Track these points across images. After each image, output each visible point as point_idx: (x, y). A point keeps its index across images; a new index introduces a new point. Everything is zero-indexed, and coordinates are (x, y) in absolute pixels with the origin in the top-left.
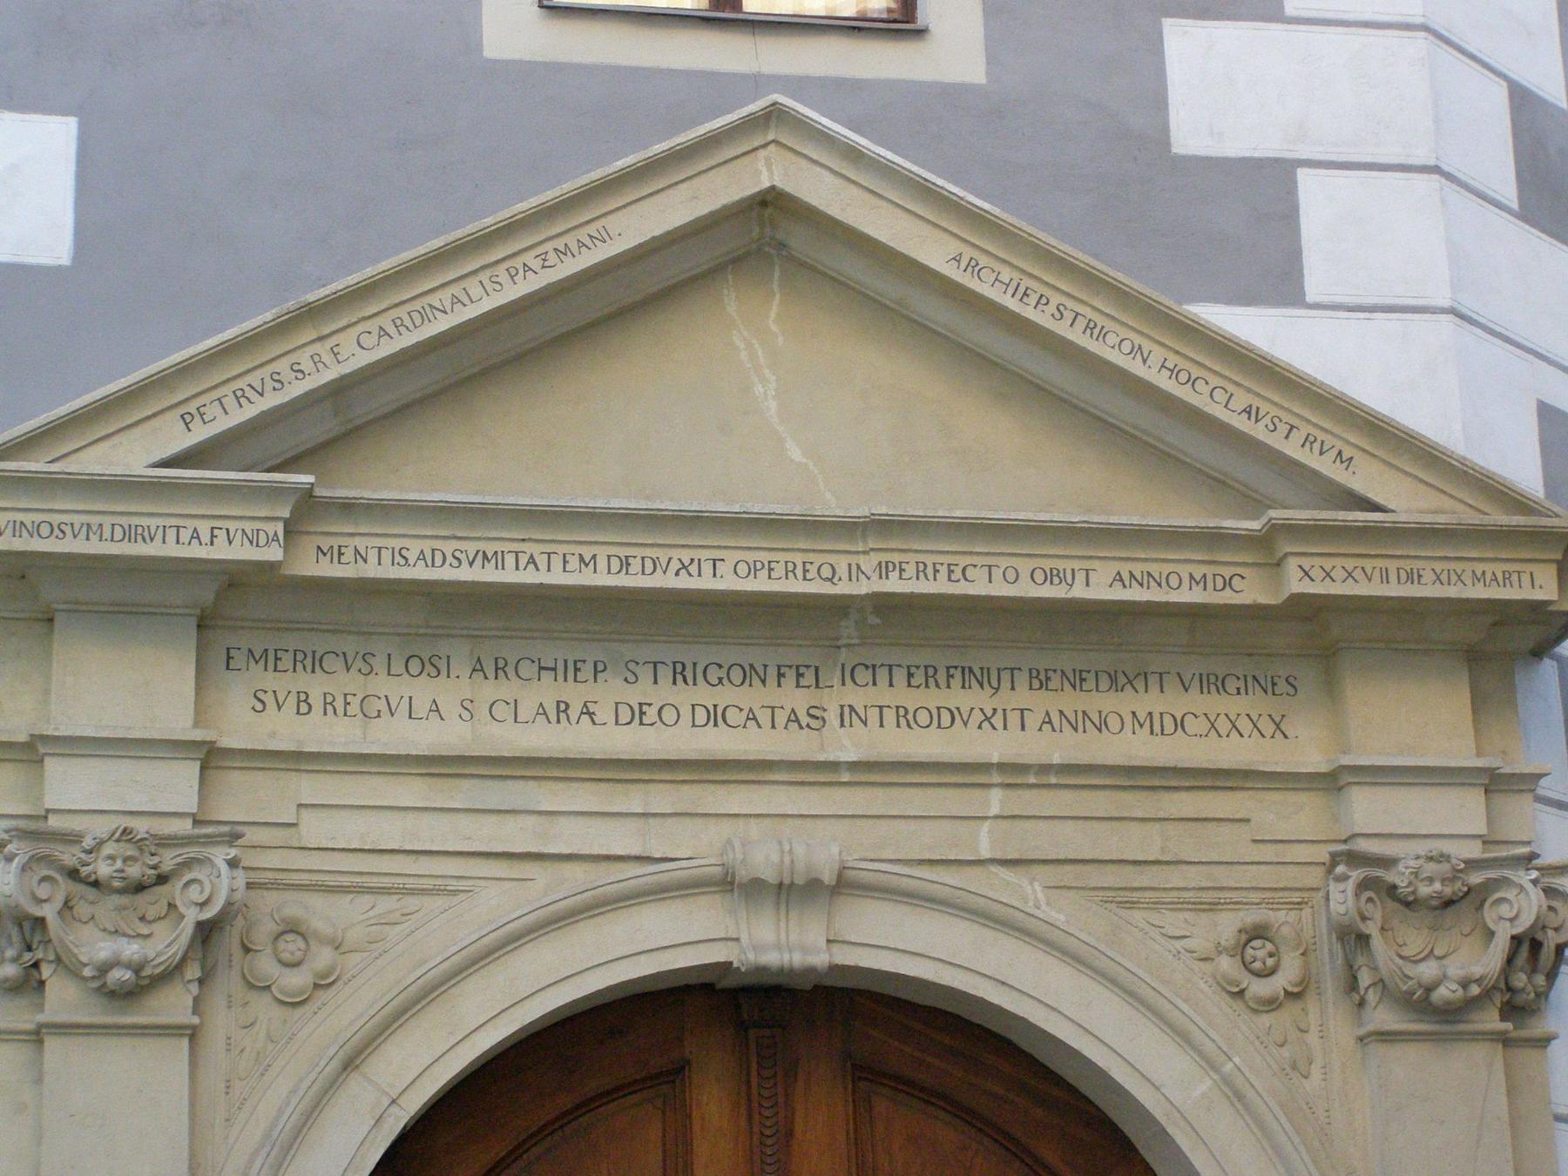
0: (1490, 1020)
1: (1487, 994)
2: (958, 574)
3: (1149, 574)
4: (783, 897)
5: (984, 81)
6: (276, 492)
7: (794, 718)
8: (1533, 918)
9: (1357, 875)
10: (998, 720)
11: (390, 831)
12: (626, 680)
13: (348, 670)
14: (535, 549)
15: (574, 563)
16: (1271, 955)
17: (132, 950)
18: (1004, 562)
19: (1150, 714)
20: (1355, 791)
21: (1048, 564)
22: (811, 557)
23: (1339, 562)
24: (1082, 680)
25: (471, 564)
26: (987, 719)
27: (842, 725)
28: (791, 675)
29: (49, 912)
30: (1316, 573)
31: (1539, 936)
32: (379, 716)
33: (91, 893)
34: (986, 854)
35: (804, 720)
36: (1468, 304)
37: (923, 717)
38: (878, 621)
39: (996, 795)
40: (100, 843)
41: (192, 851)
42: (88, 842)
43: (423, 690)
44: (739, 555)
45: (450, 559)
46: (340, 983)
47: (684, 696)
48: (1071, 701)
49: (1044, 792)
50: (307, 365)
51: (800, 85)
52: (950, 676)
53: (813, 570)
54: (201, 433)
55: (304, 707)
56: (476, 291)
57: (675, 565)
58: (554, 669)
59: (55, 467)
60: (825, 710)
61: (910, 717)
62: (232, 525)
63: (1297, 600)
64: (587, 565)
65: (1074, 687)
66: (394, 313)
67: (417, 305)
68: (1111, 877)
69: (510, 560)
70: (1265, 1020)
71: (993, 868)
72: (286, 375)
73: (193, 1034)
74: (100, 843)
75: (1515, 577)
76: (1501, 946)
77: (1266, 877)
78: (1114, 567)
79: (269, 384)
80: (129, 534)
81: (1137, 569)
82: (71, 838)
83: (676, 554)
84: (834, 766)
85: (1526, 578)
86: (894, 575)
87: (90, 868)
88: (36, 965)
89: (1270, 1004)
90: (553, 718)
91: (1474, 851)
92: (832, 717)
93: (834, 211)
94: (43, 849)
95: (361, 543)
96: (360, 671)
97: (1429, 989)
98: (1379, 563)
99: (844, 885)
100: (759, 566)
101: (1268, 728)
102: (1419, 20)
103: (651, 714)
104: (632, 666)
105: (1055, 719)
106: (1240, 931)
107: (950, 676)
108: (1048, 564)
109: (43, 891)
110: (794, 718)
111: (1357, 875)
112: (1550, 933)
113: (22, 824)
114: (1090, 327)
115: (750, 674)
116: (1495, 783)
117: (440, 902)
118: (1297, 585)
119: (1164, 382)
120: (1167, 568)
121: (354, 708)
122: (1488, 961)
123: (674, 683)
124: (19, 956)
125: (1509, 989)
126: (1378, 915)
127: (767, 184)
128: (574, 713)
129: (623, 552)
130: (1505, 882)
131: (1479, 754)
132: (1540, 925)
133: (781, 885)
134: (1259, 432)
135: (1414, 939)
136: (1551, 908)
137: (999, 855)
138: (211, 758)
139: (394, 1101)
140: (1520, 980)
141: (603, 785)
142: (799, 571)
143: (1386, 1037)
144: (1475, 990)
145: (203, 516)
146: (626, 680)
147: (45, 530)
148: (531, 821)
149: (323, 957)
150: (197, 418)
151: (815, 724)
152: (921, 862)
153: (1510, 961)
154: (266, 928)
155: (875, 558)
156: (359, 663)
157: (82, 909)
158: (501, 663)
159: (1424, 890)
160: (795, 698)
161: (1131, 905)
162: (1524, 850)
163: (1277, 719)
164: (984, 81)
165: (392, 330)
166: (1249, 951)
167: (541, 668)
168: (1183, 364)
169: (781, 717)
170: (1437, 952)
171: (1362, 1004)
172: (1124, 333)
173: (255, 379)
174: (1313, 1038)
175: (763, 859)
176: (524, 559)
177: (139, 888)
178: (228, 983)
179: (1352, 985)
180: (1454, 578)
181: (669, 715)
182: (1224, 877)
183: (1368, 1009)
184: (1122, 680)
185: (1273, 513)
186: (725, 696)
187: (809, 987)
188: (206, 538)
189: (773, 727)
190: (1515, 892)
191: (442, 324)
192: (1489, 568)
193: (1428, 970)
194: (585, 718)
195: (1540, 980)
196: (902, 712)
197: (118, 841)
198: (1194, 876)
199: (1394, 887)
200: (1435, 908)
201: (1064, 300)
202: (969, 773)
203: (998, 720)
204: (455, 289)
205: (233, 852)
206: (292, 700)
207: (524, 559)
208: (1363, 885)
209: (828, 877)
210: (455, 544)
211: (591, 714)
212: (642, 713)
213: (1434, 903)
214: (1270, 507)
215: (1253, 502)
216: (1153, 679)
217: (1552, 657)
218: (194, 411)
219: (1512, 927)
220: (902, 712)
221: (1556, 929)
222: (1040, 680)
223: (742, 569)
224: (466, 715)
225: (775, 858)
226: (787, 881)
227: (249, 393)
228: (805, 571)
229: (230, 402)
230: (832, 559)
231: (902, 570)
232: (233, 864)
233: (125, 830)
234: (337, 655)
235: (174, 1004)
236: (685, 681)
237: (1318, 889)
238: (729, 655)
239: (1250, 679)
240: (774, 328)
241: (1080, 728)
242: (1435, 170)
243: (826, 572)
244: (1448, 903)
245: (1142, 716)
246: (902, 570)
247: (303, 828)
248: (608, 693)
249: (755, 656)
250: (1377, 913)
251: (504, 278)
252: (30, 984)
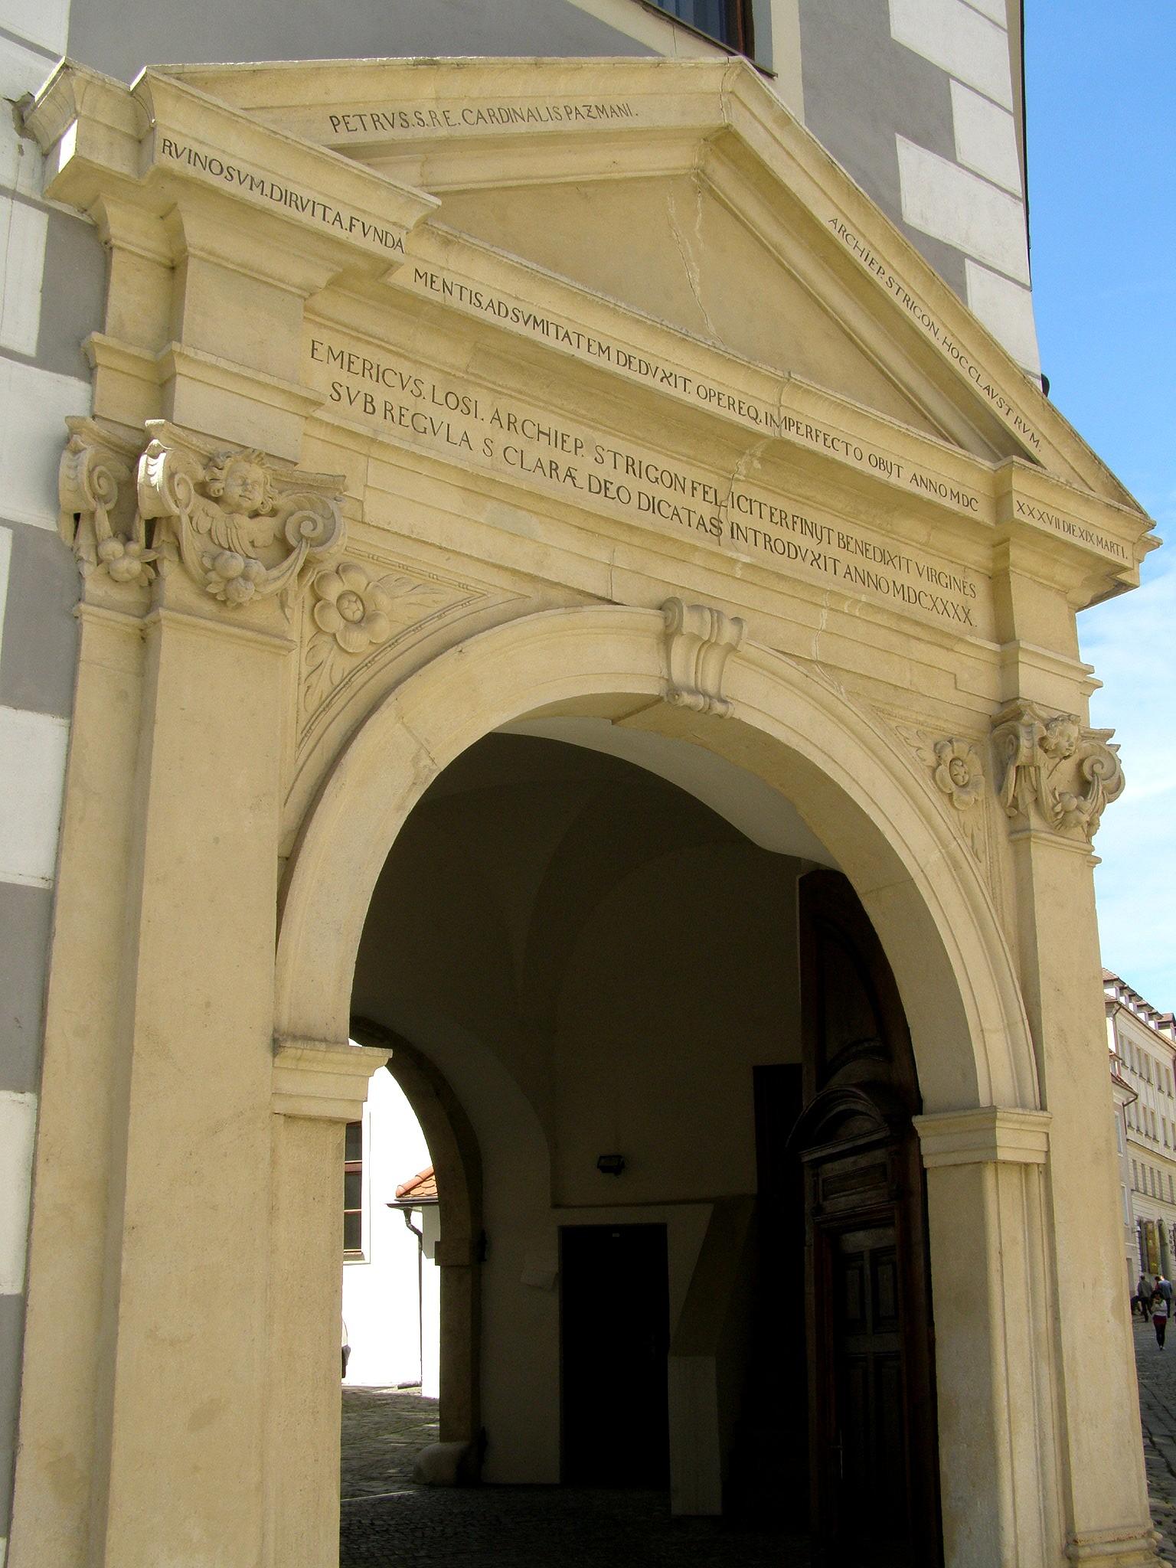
2: (829, 443)
7: (701, 522)
12: (596, 459)
19: (903, 585)
27: (732, 537)
32: (425, 432)
35: (709, 526)
38: (759, 466)
45: (511, 314)
55: (369, 408)
60: (722, 523)
61: (772, 543)
64: (604, 352)
96: (412, 391)
100: (712, 394)
121: (407, 420)
146: (596, 459)
150: (342, 123)
151: (714, 530)
156: (411, 386)
167: (540, 432)
172: (926, 311)
186: (661, 492)
201: (895, 277)
206: (361, 397)
211: (573, 478)
218: (341, 119)
228: (740, 408)
234: (396, 374)
239: (952, 579)
245: (898, 586)
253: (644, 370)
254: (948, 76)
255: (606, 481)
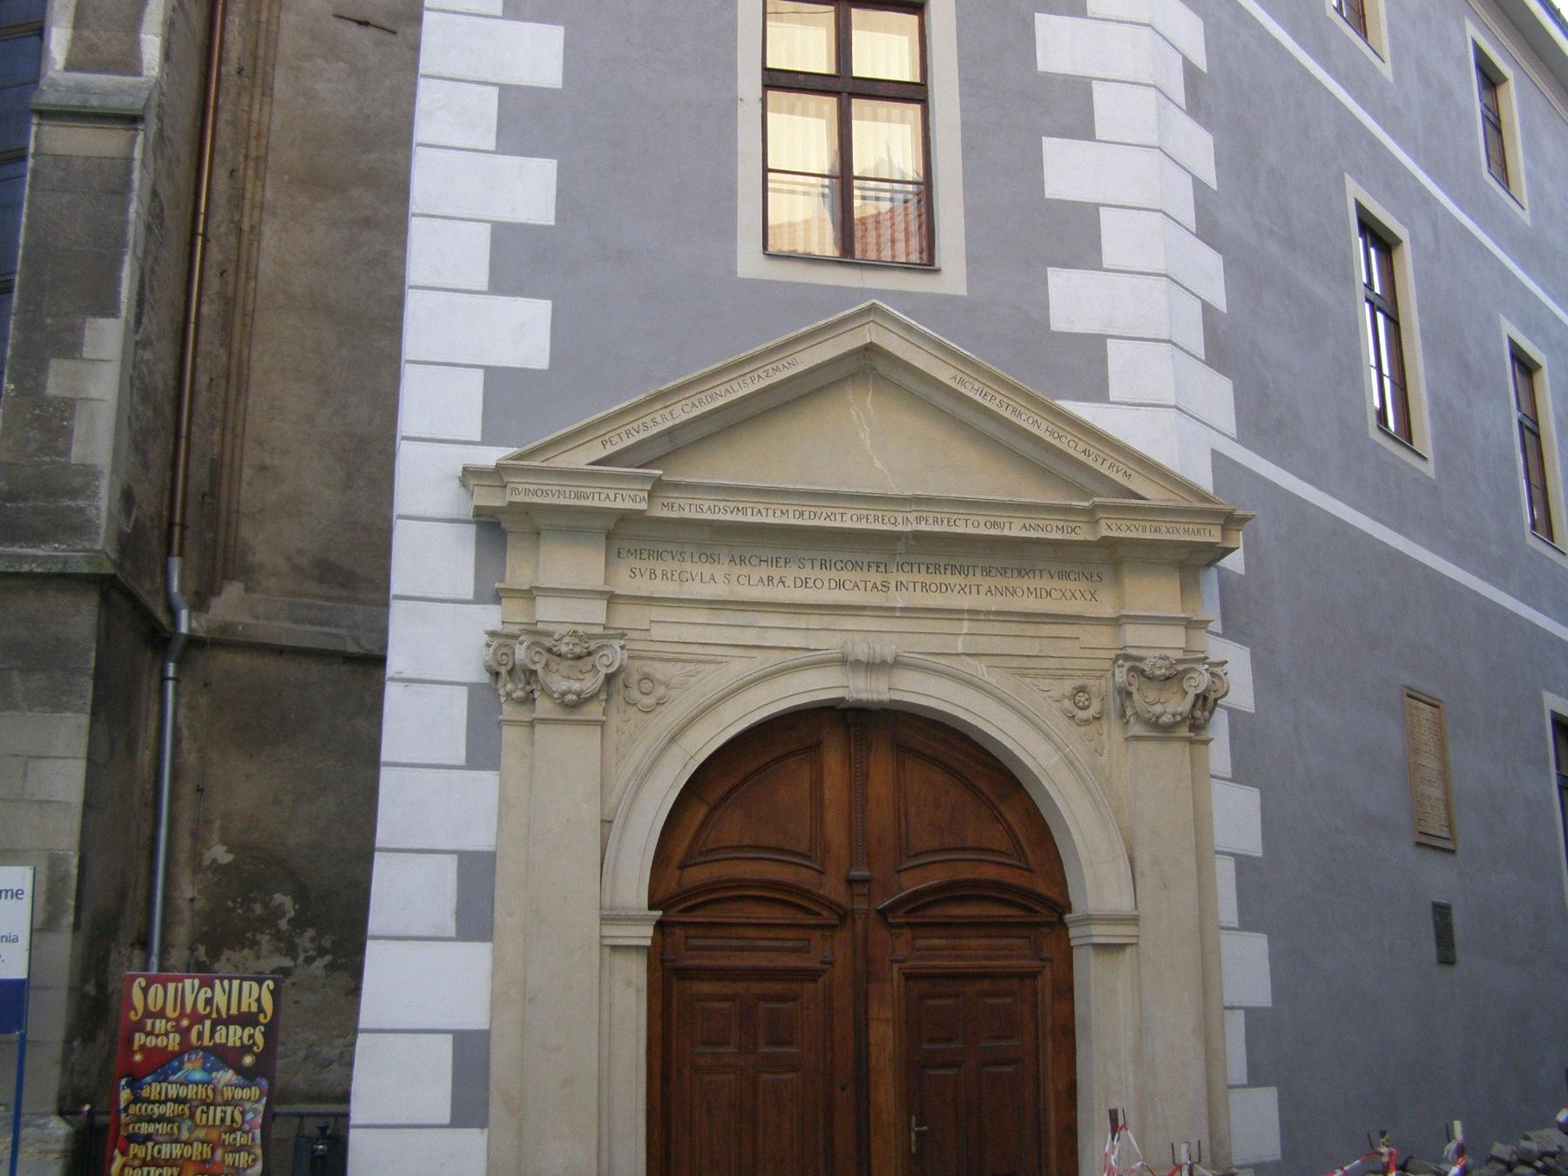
0: (1184, 732)
1: (1183, 720)
3: (1038, 526)
4: (869, 667)
5: (966, 294)
6: (645, 478)
7: (875, 586)
8: (1205, 686)
9: (1128, 665)
10: (967, 590)
11: (692, 634)
13: (673, 559)
14: (761, 507)
15: (778, 513)
16: (1087, 700)
17: (576, 686)
18: (973, 518)
19: (1036, 589)
20: (1127, 626)
21: (992, 519)
22: (885, 513)
23: (1124, 522)
24: (1005, 572)
25: (732, 513)
26: (962, 589)
27: (897, 590)
28: (874, 566)
29: (538, 668)
30: (1114, 527)
31: (1207, 695)
33: (558, 659)
34: (960, 650)
35: (880, 587)
36: (1182, 404)
37: (933, 587)
39: (966, 624)
40: (562, 637)
41: (604, 642)
42: (556, 636)
43: (707, 569)
44: (852, 512)
45: (722, 510)
46: (667, 703)
47: (826, 575)
48: (1000, 582)
49: (987, 623)
50: (658, 419)
51: (881, 294)
52: (946, 569)
53: (886, 519)
54: (610, 450)
55: (653, 576)
56: (736, 387)
57: (824, 515)
58: (767, 561)
59: (545, 464)
61: (927, 587)
62: (624, 493)
63: (1104, 539)
65: (1001, 575)
66: (698, 396)
67: (709, 393)
68: (1017, 663)
69: (749, 511)
70: (1083, 729)
71: (963, 657)
72: (650, 424)
73: (602, 724)
74: (562, 637)
75: (1202, 531)
76: (1190, 698)
77: (1085, 664)
78: (1023, 521)
79: (642, 428)
80: (577, 496)
81: (1033, 523)
82: (548, 634)
83: (825, 510)
84: (893, 609)
85: (1207, 532)
86: (923, 523)
87: (556, 649)
88: (532, 692)
89: (1086, 722)
90: (766, 583)
91: (1180, 655)
92: (892, 586)
93: (899, 354)
94: (537, 638)
95: (682, 502)
97: (1158, 718)
98: (1143, 523)
99: (897, 664)
101: (1088, 596)
102: (1164, 272)
103: (810, 583)
104: (802, 561)
105: (993, 589)
106: (1074, 688)
107: (946, 569)
108: (992, 519)
109: (536, 658)
110: (875, 586)
111: (1128, 665)
112: (1212, 693)
113: (527, 627)
114: (1014, 411)
115: (856, 566)
116: (1190, 624)
117: (713, 666)
118: (1105, 533)
119: (1047, 437)
120: (1046, 522)
122: (1185, 706)
123: (821, 568)
124: (525, 687)
125: (1193, 717)
126: (1136, 684)
127: (869, 341)
128: (775, 582)
129: (801, 509)
130: (1194, 670)
131: (1183, 611)
132: (1208, 690)
133: (868, 663)
134: (1090, 461)
135: (1152, 695)
136: (1213, 682)
137: (965, 652)
138: (612, 598)
139: (692, 757)
140: (1198, 714)
141: (788, 615)
142: (880, 519)
143: (1137, 738)
144: (1179, 718)
145: (612, 488)
147: (539, 493)
148: (754, 631)
149: (661, 691)
152: (931, 654)
153: (1194, 706)
154: (635, 677)
155: (915, 514)
157: (553, 667)
158: (743, 558)
159: (1158, 672)
160: (876, 577)
161: (1025, 675)
162: (1202, 655)
163: (1093, 592)
164: (966, 294)
165: (697, 404)
166: (1077, 698)
168: (1056, 429)
169: (869, 586)
170: (1161, 701)
171: (1127, 722)
172: (1029, 414)
173: (634, 425)
174: (1105, 737)
175: (861, 651)
176: (756, 511)
177: (579, 657)
178: (618, 701)
179: (1123, 714)
180: (1175, 531)
181: (819, 584)
182: (1067, 664)
183: (1130, 725)
184: (1023, 572)
185: (1096, 499)
186: (845, 575)
187: (878, 708)
188: (612, 498)
189: (866, 590)
190: (1197, 674)
191: (720, 402)
192: (1191, 526)
193: (1158, 709)
194: (781, 584)
195: (1207, 714)
196: (924, 585)
197: (571, 636)
198: (1053, 663)
199: (1144, 670)
200: (1161, 681)
202: (955, 614)
203: (967, 590)
204: (727, 386)
205: (622, 642)
206: (648, 573)
207: (756, 511)
208: (1131, 669)
209: (890, 660)
210: (726, 503)
211: (783, 582)
212: (806, 582)
213: (1162, 678)
214: (1093, 496)
215: (1085, 493)
216: (1037, 573)
217: (1215, 567)
219: (1196, 689)
220: (924, 585)
221: (1215, 691)
222: (987, 572)
223: (855, 518)
224: (727, 581)
225: (867, 651)
226: (871, 661)
227: (632, 431)
228: (883, 519)
229: (624, 436)
230: (895, 514)
231: (927, 520)
232: (622, 647)
233: (574, 631)
235: (594, 711)
236: (826, 568)
237: (1109, 671)
238: (846, 556)
240: (869, 407)
241: (1004, 594)
242: (1169, 341)
243: (893, 520)
244: (1167, 678)
246: (927, 520)
247: (652, 631)
248: (791, 573)
249: (858, 557)
250: (1135, 682)
251: (749, 381)
252: (529, 700)
253: (812, 517)
254: (1097, 206)
255: (806, 579)
